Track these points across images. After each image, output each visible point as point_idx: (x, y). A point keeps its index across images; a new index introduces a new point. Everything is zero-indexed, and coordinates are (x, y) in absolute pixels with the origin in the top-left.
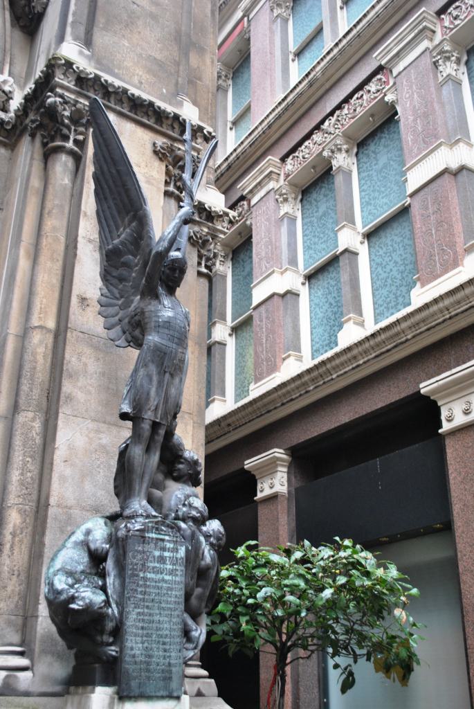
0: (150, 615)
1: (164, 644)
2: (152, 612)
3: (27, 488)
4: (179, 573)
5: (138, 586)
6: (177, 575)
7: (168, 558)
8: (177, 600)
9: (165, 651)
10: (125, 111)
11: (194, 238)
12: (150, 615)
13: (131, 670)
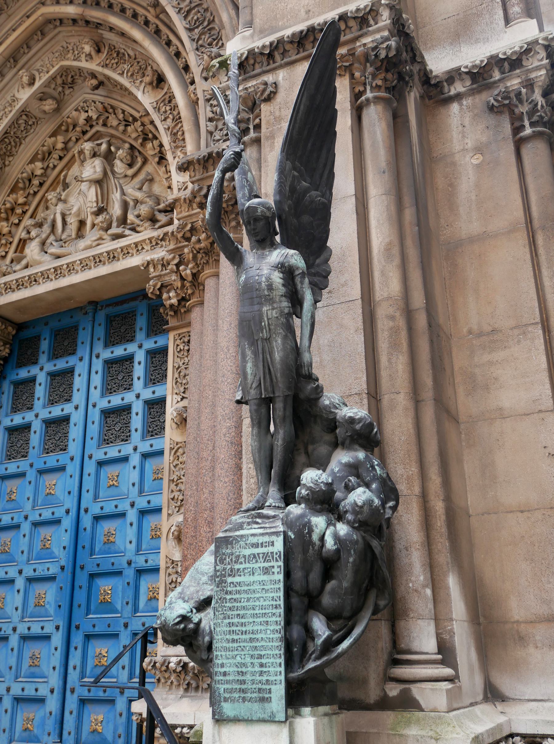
0: (242, 624)
1: (260, 657)
2: (243, 620)
3: (252, 495)
4: (276, 570)
5: (226, 593)
6: (273, 573)
7: (261, 555)
8: (274, 603)
9: (261, 665)
10: (294, 58)
11: (496, 104)
12: (242, 624)
13: (222, 689)
